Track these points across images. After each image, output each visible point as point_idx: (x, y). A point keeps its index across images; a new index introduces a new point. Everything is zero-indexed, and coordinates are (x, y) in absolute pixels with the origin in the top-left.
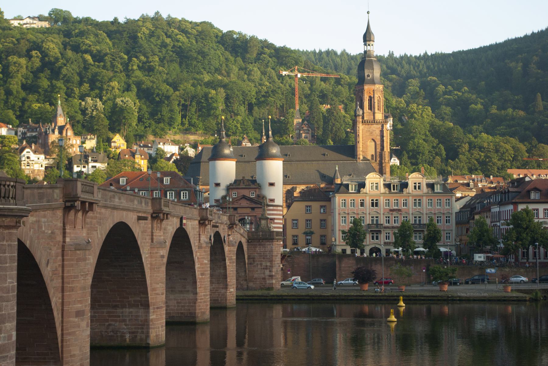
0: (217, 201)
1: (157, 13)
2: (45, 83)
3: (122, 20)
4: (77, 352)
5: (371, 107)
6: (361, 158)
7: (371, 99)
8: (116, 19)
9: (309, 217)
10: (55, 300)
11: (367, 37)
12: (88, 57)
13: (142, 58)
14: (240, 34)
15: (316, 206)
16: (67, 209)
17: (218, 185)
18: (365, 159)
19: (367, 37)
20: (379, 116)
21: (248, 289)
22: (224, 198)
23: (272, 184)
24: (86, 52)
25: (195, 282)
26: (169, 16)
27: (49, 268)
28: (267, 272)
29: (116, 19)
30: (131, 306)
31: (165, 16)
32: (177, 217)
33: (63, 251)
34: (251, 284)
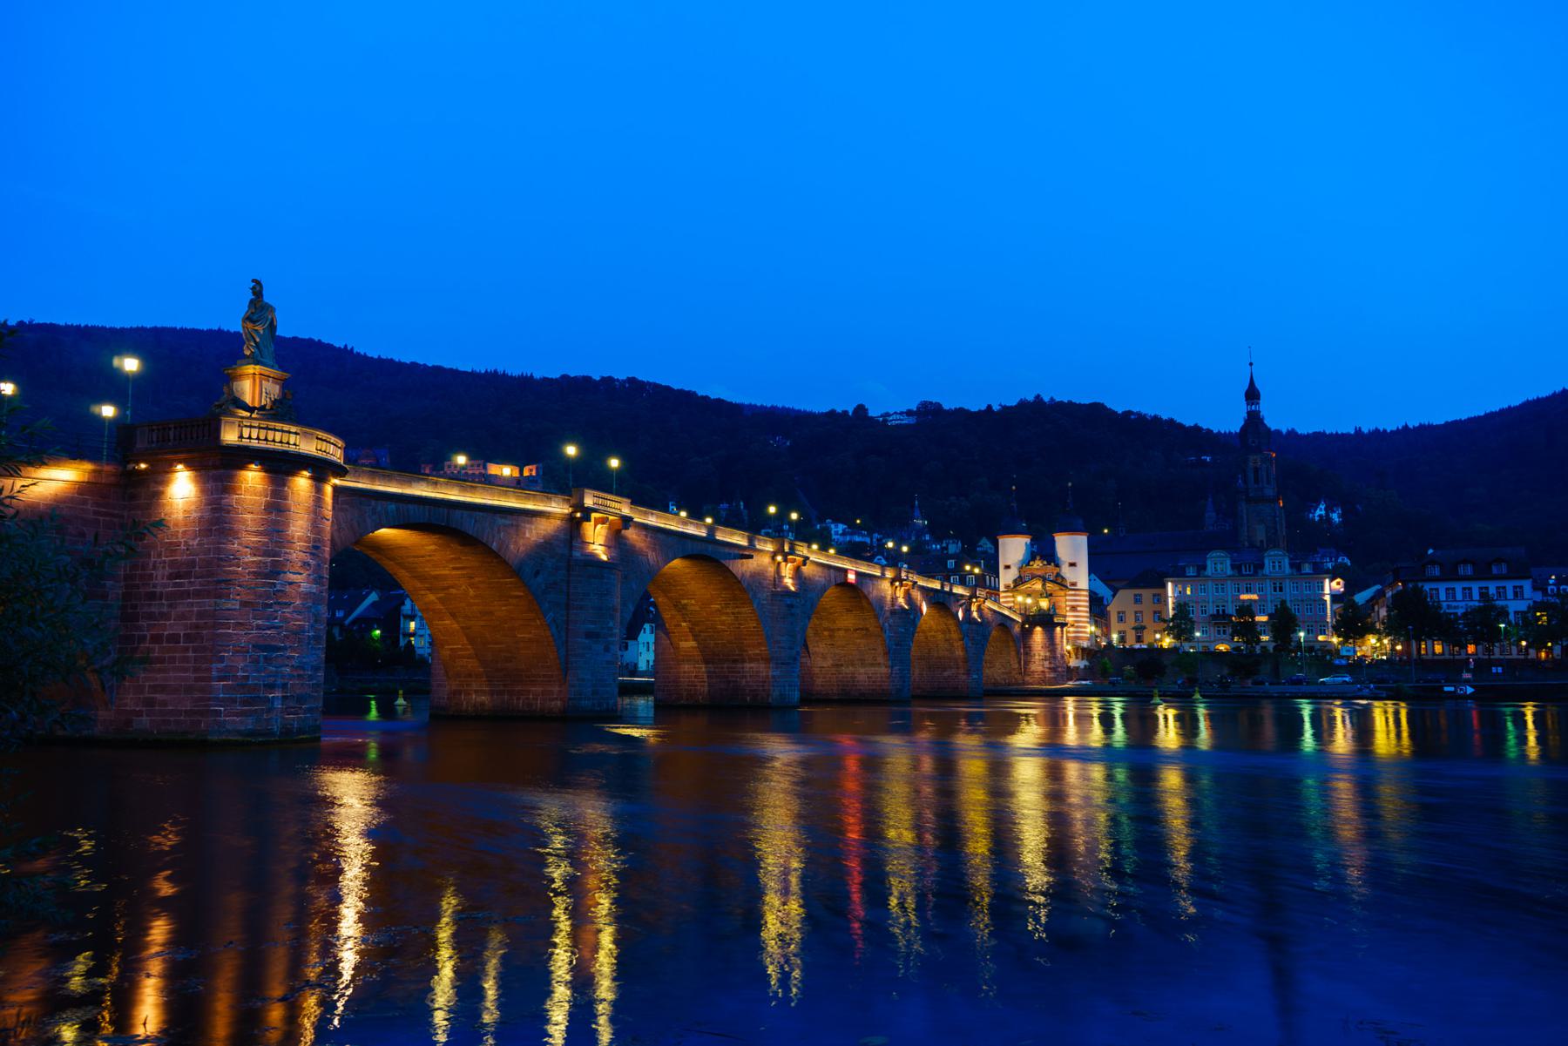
1: (1038, 396)
3: (996, 408)
5: (1256, 481)
7: (1256, 470)
8: (989, 407)
11: (1252, 395)
15: (1147, 594)
17: (1008, 567)
19: (1252, 395)
20: (1270, 492)
21: (1024, 683)
23: (1072, 565)
27: (540, 579)
29: (989, 407)
30: (751, 660)
31: (1046, 399)
34: (1027, 678)
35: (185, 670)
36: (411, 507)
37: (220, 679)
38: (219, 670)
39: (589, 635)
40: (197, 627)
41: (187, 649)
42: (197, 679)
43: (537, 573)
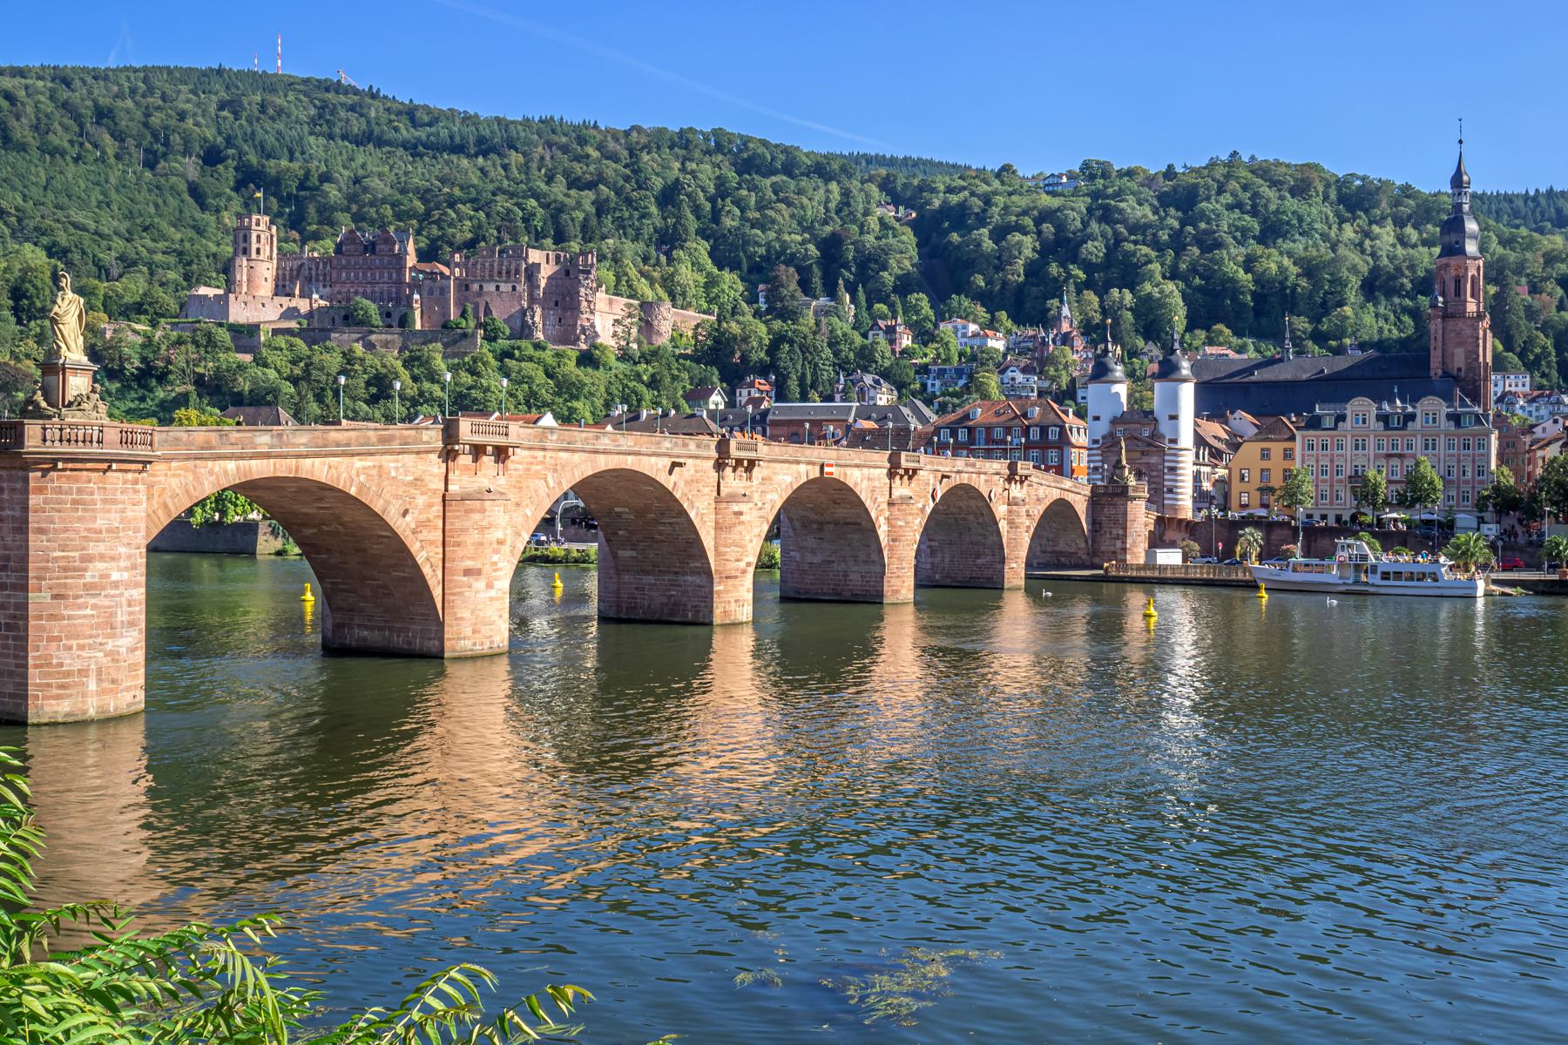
0: (1096, 442)
2: (1054, 269)
4: (466, 614)
6: (1440, 372)
8: (1170, 167)
9: (1266, 464)
10: (426, 556)
12: (1121, 228)
13: (1203, 225)
14: (1363, 179)
16: (448, 455)
17: (1097, 418)
18: (1446, 374)
22: (1104, 437)
24: (1118, 222)
25: (880, 551)
26: (1252, 158)
27: (408, 518)
28: (1119, 544)
29: (1170, 167)
32: (809, 463)
33: (444, 500)
35: (7, 656)
36: (253, 462)
37: (36, 666)
38: (35, 658)
39: (467, 572)
40: (14, 617)
41: (7, 637)
42: (17, 666)
43: (405, 513)
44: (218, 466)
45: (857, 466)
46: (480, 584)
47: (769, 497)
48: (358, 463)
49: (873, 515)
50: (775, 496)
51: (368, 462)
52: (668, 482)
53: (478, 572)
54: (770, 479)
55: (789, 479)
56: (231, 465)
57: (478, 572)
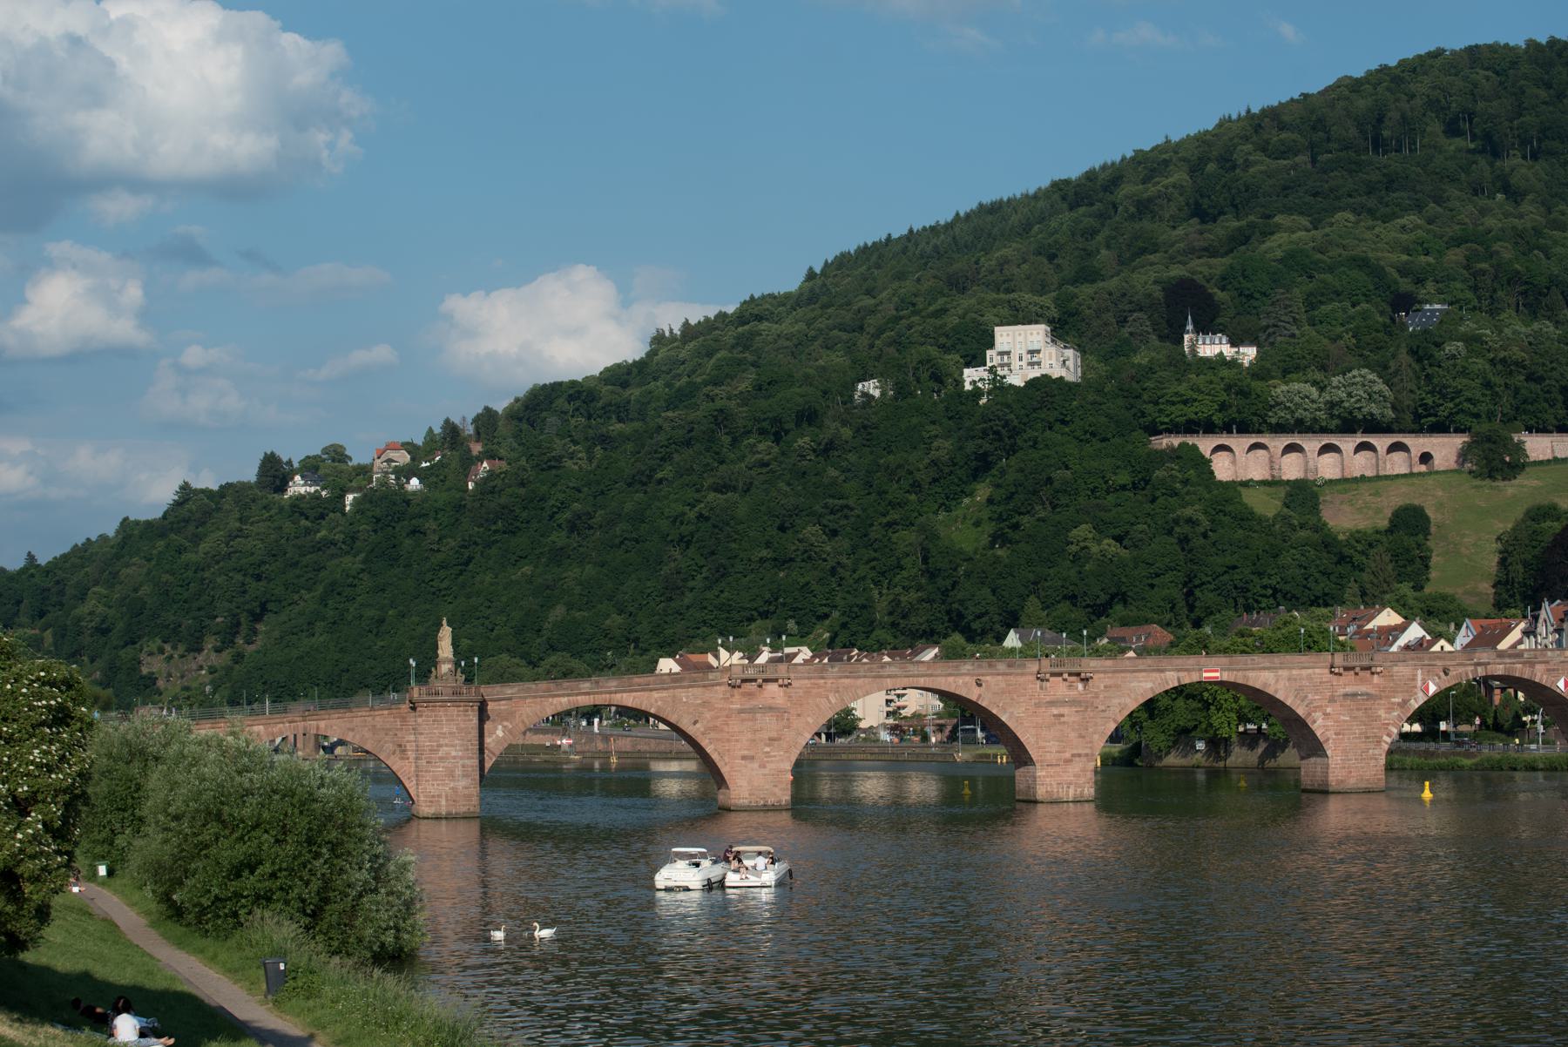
39: (744, 758)
43: (695, 722)
44: (556, 700)
45: (1268, 669)
46: (756, 765)
47: (1116, 701)
48: (655, 695)
49: (1301, 711)
50: (1128, 700)
51: (664, 694)
52: (973, 694)
53: (752, 758)
54: (1117, 686)
55: (1149, 685)
56: (564, 700)
57: (752, 758)
